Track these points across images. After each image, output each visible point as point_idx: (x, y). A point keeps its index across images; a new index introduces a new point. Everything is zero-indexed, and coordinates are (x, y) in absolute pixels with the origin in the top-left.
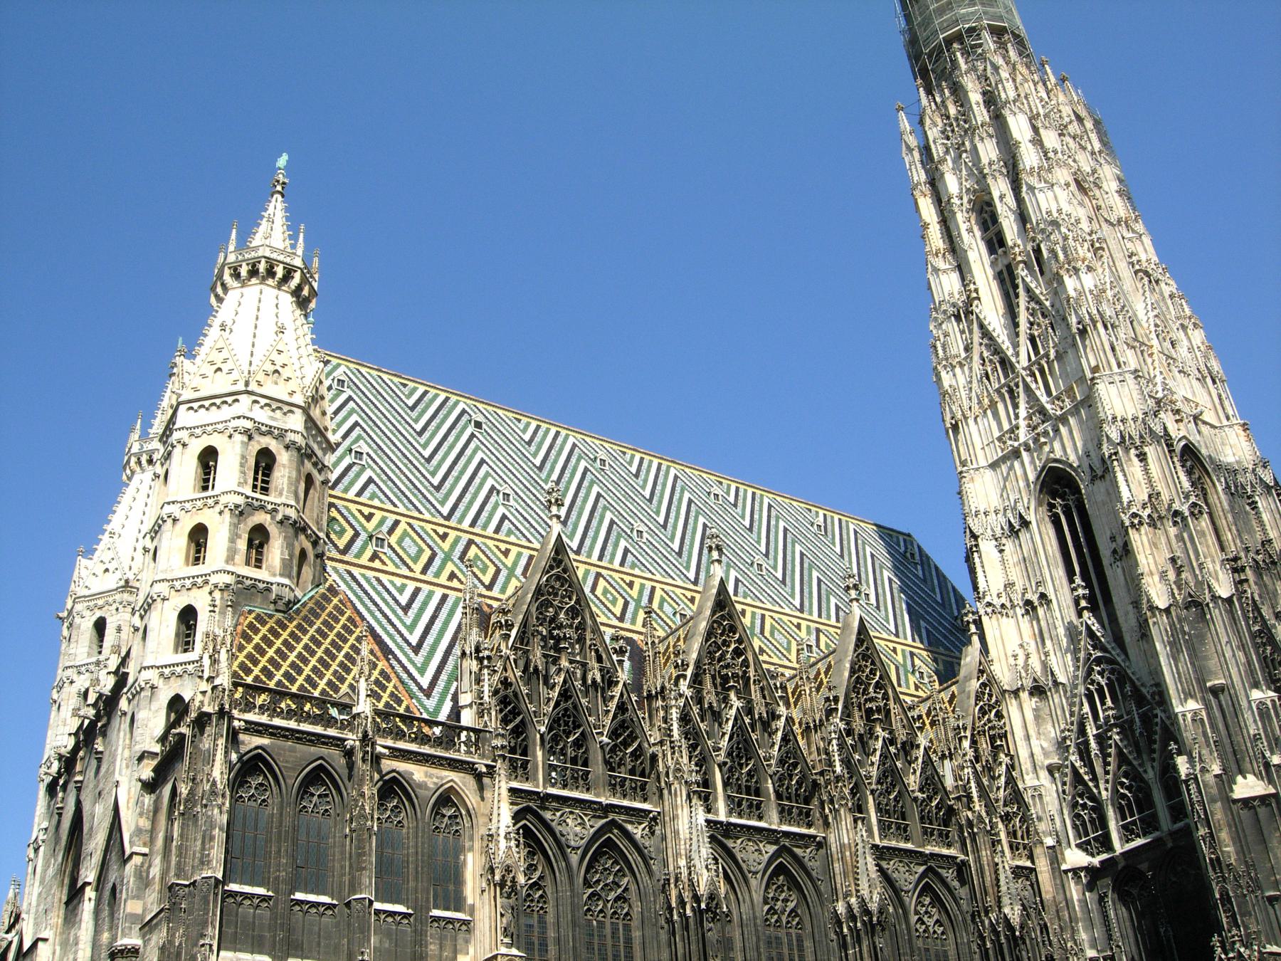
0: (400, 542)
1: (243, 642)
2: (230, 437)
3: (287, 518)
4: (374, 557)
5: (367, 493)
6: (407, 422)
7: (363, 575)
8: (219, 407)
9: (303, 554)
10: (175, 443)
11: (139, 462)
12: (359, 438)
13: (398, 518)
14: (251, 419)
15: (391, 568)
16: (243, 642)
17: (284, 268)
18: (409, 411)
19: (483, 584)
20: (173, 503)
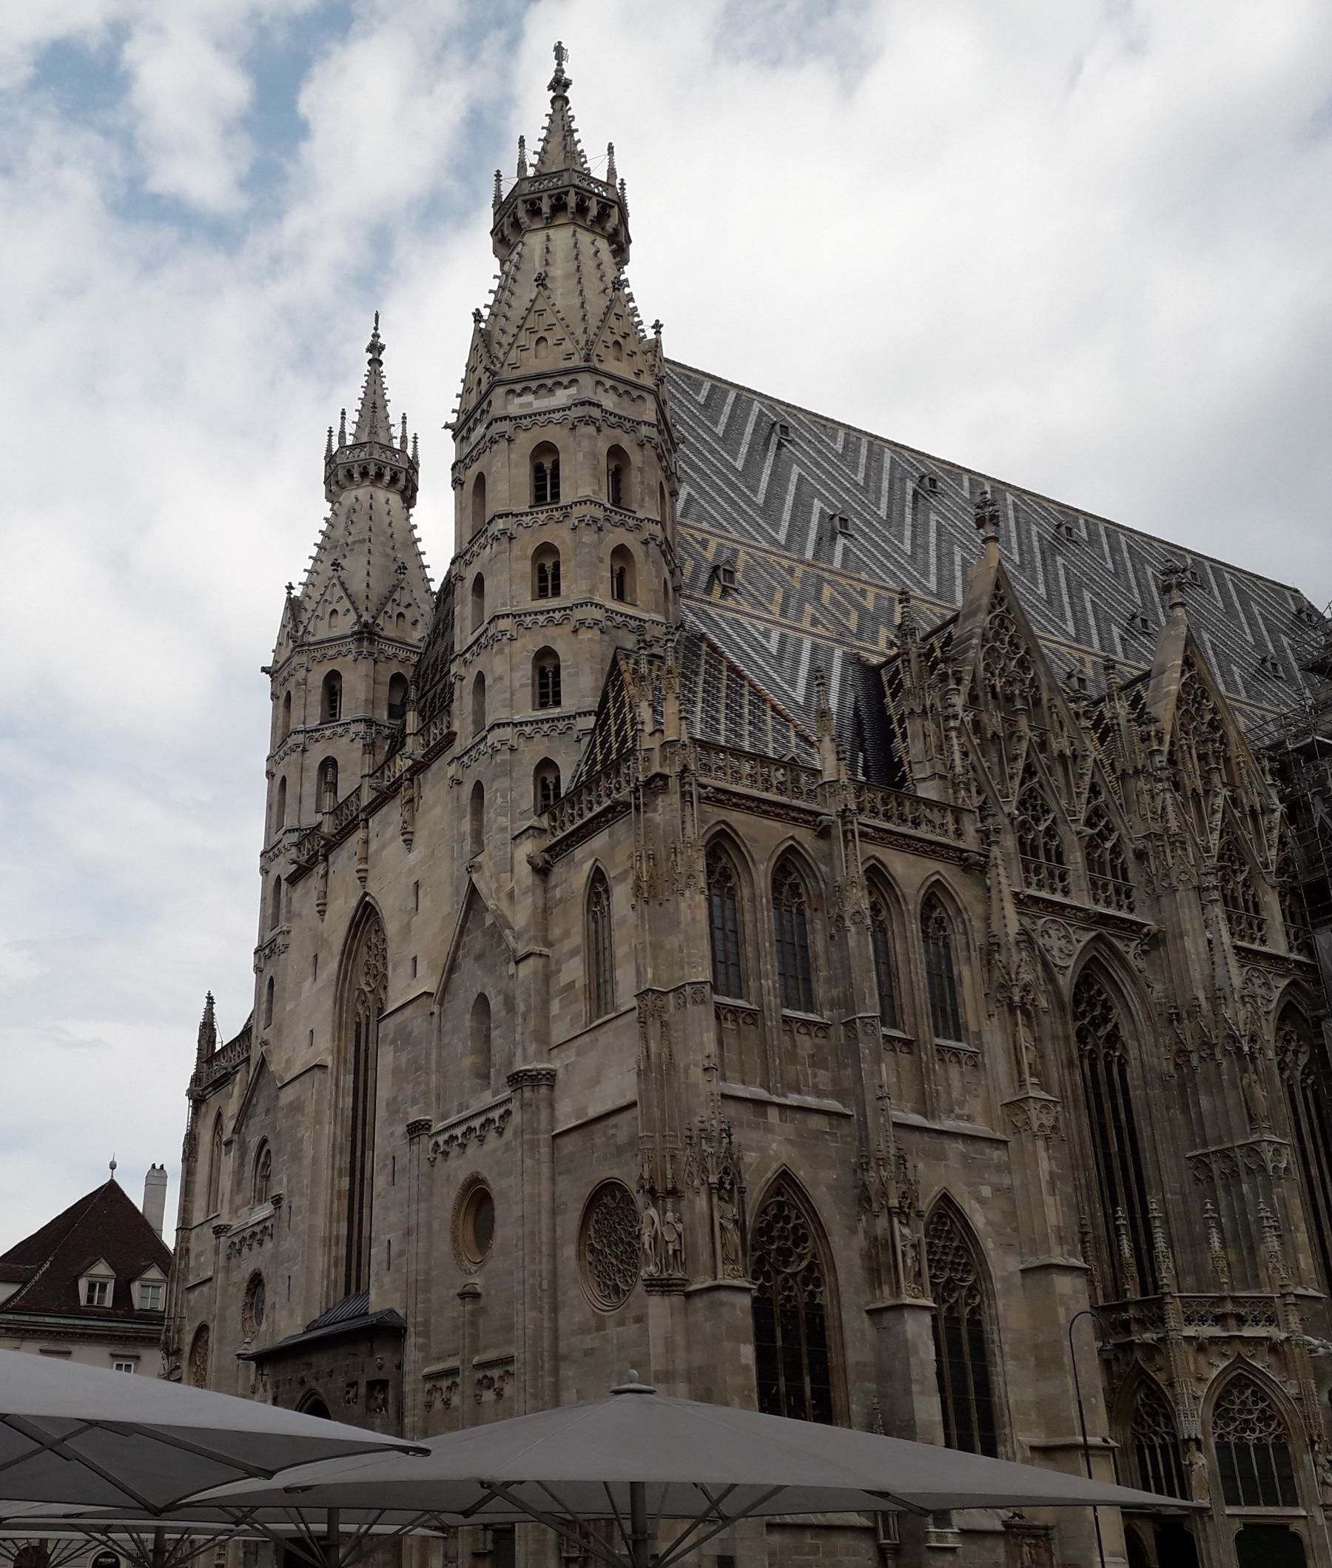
0: (746, 576)
2: (574, 428)
4: (725, 592)
7: (721, 616)
10: (497, 437)
11: (350, 475)
13: (738, 546)
14: (599, 406)
15: (749, 609)
17: (598, 202)
19: (847, 628)
20: (507, 515)
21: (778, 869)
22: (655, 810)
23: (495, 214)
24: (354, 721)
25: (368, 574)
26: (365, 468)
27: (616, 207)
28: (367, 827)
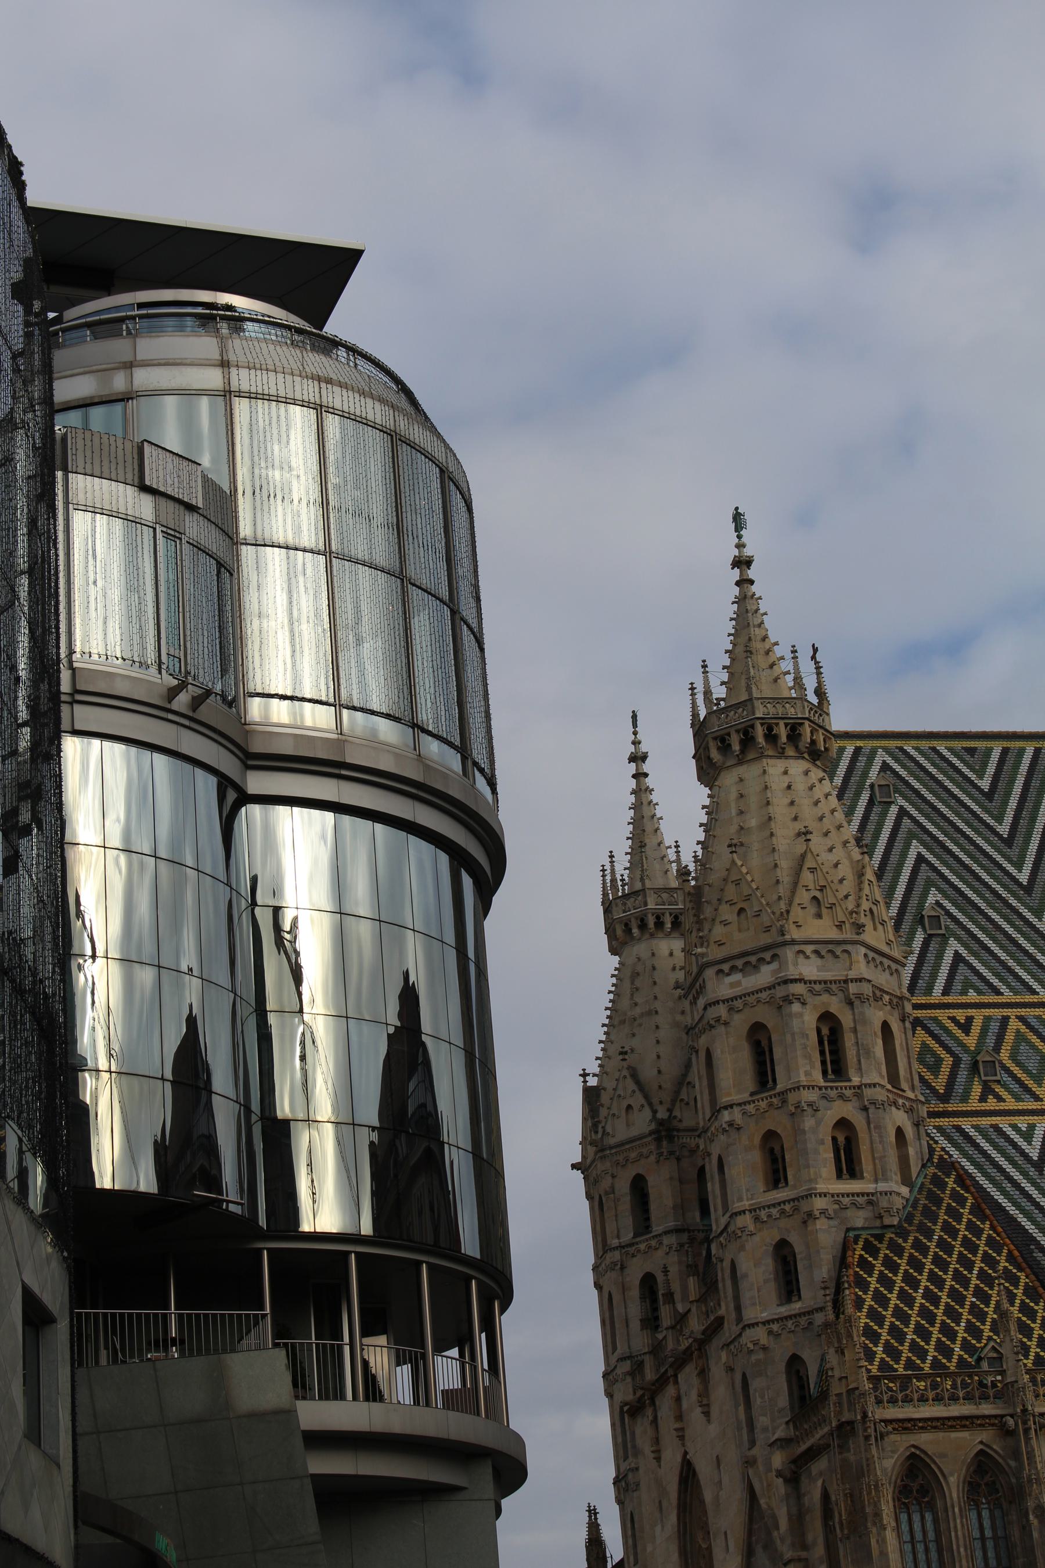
0: (1013, 1057)
1: (860, 1293)
2: (780, 1007)
3: (873, 1103)
4: (987, 1091)
5: (957, 986)
6: (988, 826)
8: (755, 967)
9: (900, 1132)
10: (712, 1022)
11: (628, 930)
12: (929, 884)
13: (1006, 1012)
15: (1011, 1104)
16: (860, 1293)
17: (786, 725)
18: (987, 803)
20: (731, 1106)
21: (975, 1471)
22: (849, 1450)
23: (694, 736)
24: (666, 1233)
25: (658, 1057)
26: (642, 920)
27: (807, 723)
28: (676, 1382)
